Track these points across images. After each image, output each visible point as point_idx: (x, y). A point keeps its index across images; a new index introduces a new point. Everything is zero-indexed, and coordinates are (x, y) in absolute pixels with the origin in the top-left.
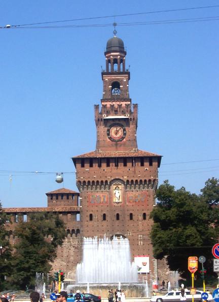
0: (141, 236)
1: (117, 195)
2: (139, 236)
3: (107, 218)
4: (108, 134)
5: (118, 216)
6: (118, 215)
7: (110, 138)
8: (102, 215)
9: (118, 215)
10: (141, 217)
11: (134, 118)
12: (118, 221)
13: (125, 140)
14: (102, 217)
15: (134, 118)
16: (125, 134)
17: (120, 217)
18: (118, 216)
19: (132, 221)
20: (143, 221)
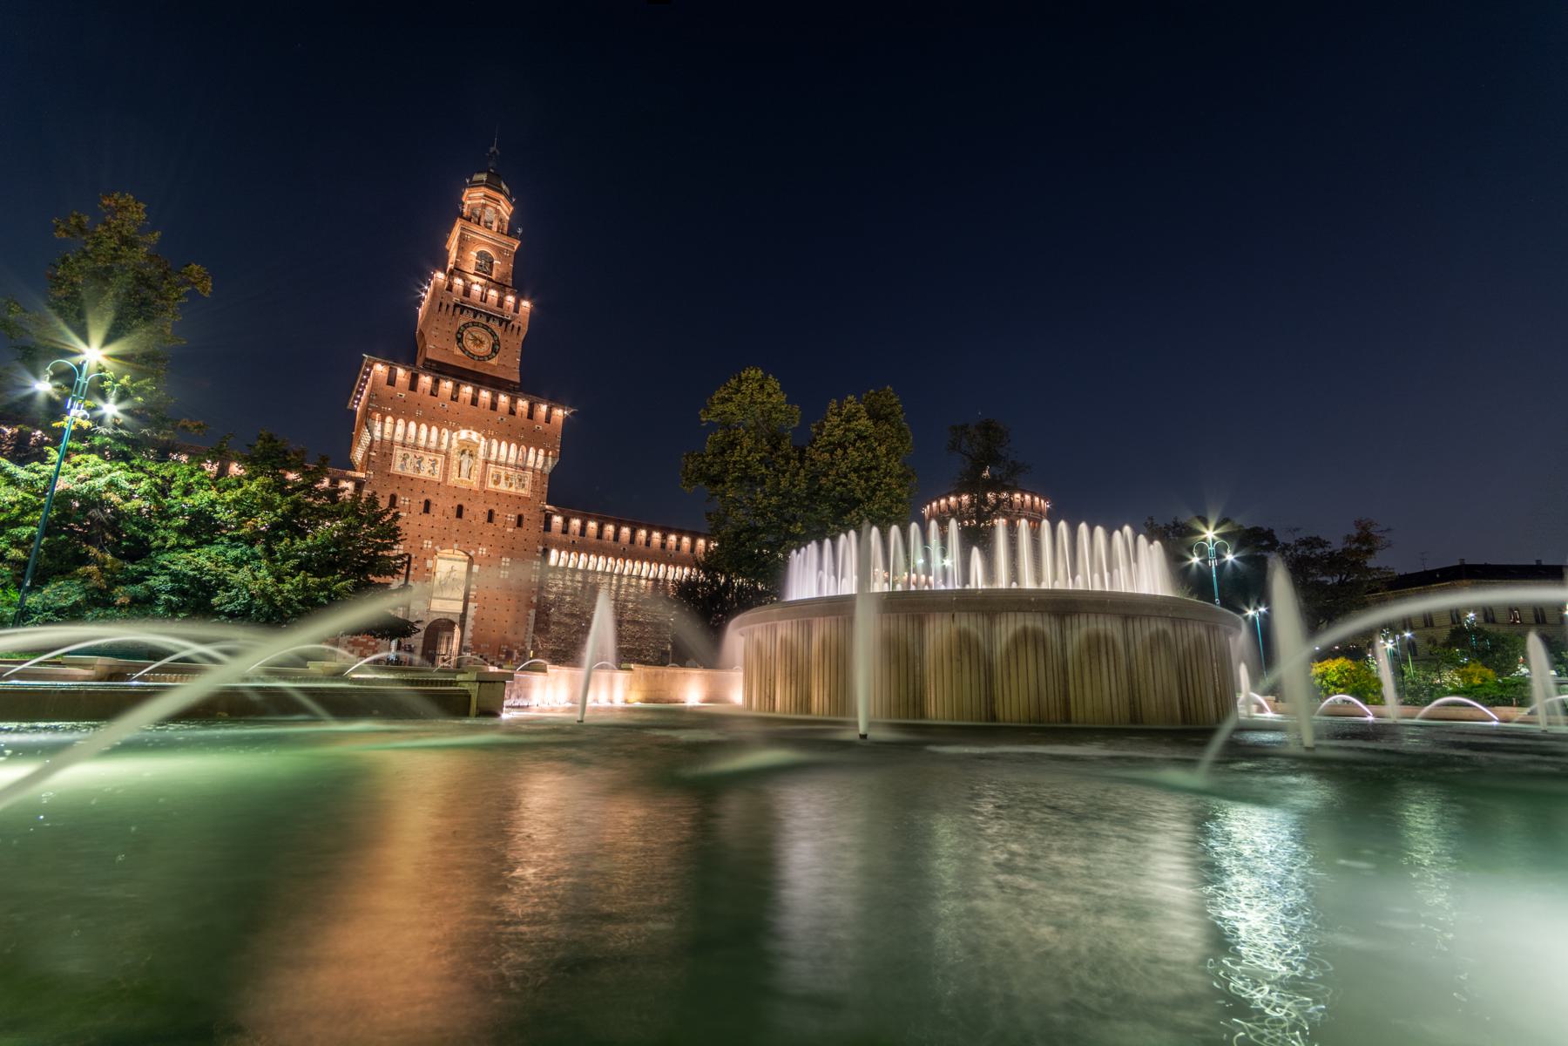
0: (508, 560)
1: (465, 466)
2: (504, 559)
3: (432, 508)
4: (460, 340)
5: (460, 511)
6: (460, 508)
7: (464, 350)
8: (423, 500)
9: (460, 508)
10: (512, 518)
11: (519, 328)
12: (459, 519)
13: (493, 362)
14: (422, 506)
15: (519, 328)
16: (495, 351)
17: (465, 513)
18: (460, 511)
19: (493, 525)
20: (517, 529)
